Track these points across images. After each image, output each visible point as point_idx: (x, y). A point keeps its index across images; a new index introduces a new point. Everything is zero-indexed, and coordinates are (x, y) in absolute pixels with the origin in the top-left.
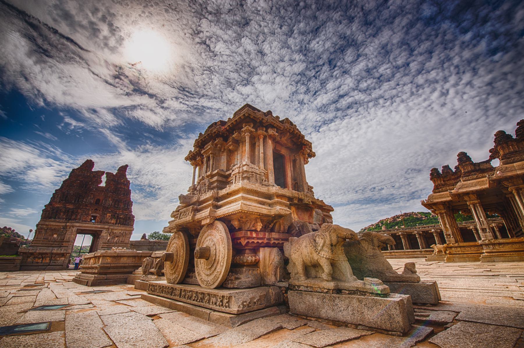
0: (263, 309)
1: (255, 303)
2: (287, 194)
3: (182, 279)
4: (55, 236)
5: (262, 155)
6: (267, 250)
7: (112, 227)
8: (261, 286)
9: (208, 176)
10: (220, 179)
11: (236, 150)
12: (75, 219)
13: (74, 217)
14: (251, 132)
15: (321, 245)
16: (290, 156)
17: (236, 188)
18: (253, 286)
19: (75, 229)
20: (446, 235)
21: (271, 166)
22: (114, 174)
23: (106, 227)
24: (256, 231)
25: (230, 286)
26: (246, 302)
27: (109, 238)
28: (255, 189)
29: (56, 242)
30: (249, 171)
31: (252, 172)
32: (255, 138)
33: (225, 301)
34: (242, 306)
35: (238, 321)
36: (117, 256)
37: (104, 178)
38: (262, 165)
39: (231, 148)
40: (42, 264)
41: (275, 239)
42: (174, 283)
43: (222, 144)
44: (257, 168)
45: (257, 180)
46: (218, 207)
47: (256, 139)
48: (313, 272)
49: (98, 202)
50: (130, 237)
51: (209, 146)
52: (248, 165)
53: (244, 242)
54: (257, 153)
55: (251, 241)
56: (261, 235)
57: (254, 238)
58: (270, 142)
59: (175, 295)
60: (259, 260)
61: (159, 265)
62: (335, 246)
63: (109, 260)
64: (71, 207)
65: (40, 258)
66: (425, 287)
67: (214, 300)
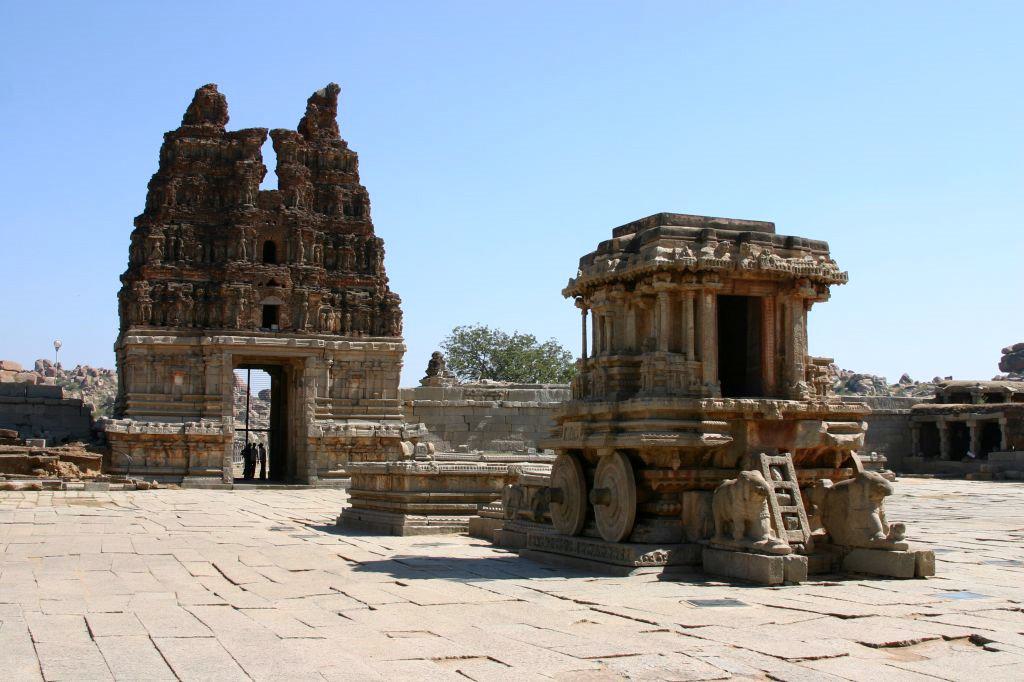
4: (178, 380)
5: (691, 333)
6: (694, 495)
10: (625, 370)
11: (651, 306)
13: (214, 314)
19: (226, 357)
24: (671, 469)
25: (638, 540)
37: (269, 155)
38: (691, 354)
41: (707, 479)
43: (624, 300)
46: (622, 431)
49: (270, 254)
51: (600, 295)
53: (655, 486)
55: (665, 484)
56: (683, 474)
57: (670, 479)
59: (571, 550)
60: (681, 511)
61: (536, 502)
65: (157, 451)
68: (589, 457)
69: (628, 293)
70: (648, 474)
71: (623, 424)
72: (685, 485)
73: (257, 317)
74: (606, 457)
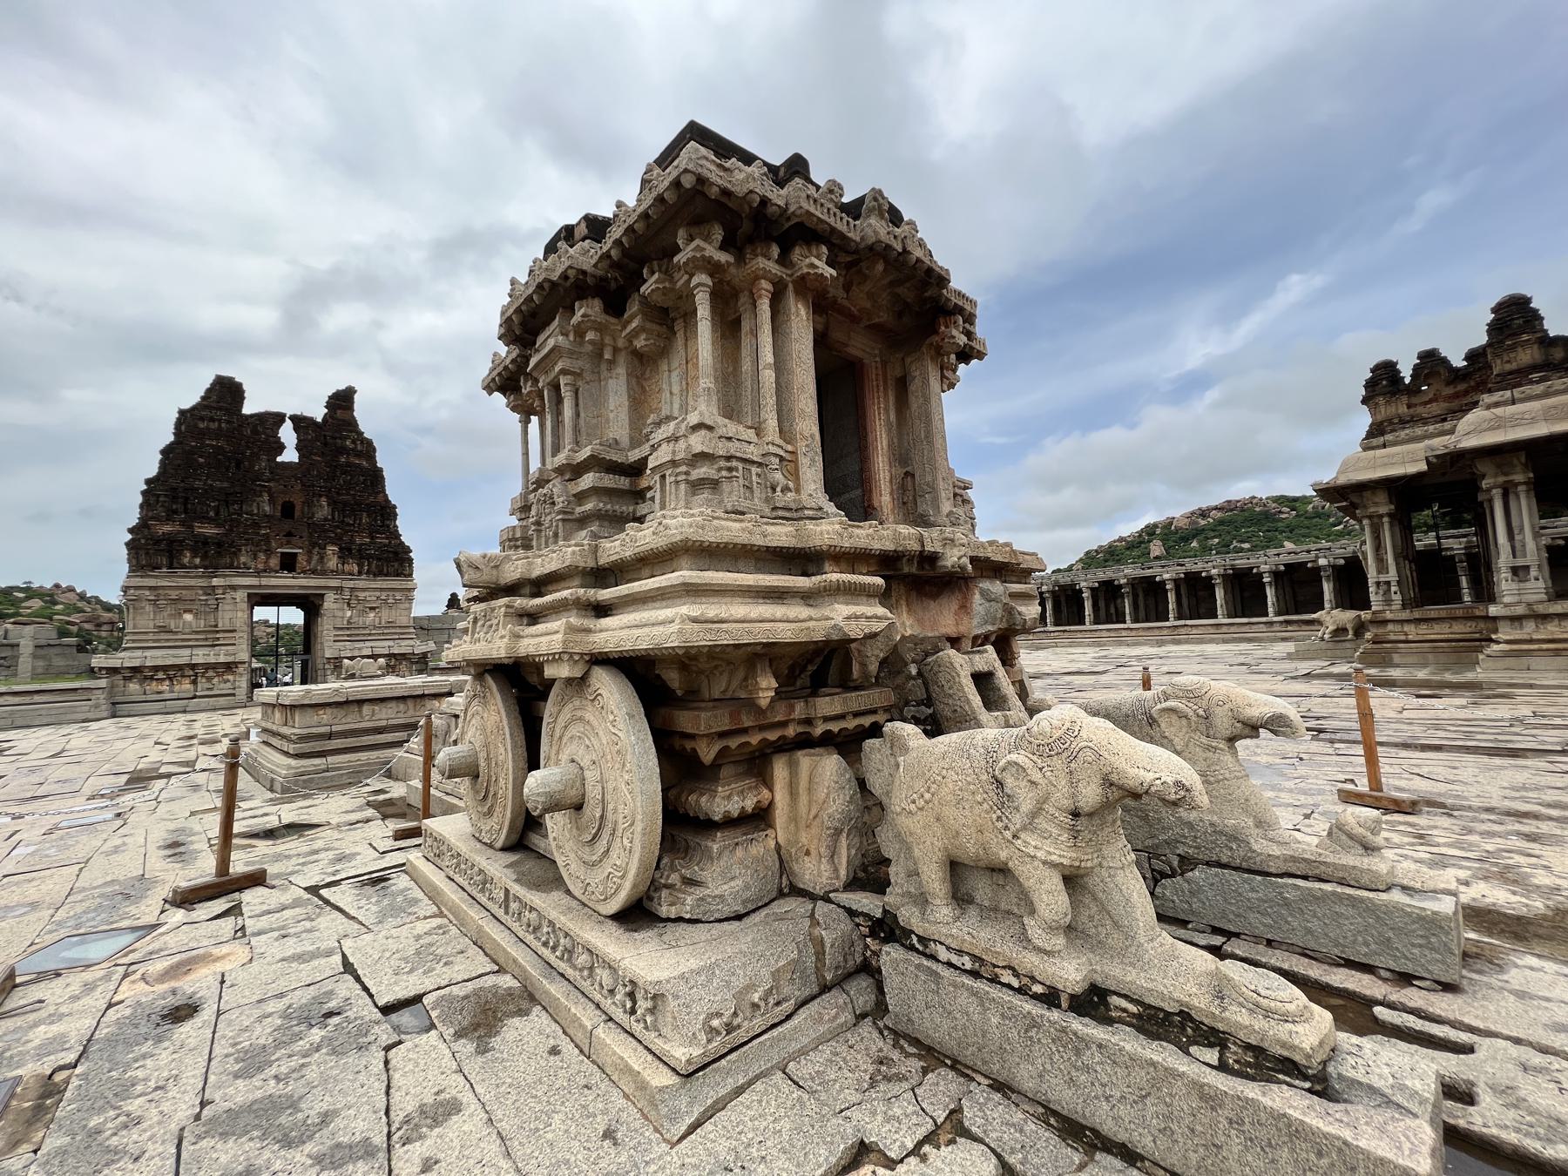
0: (789, 1017)
1: (755, 1006)
2: (877, 546)
3: (515, 837)
4: (188, 617)
5: (768, 376)
6: (805, 759)
7: (351, 584)
8: (781, 894)
9: (560, 471)
11: (664, 352)
12: (231, 566)
14: (714, 269)
15: (1026, 806)
16: (884, 364)
17: (660, 542)
18: (751, 907)
19: (241, 595)
20: (1378, 584)
21: (808, 424)
22: (319, 420)
23: (334, 583)
24: (751, 704)
26: (719, 1015)
27: (349, 614)
28: (744, 539)
29: (197, 633)
30: (730, 410)
31: (729, 458)
32: (735, 294)
33: (643, 1005)
34: (703, 1037)
35: (691, 1104)
36: (347, 702)
37: (287, 434)
38: (772, 423)
39: (640, 343)
40: (175, 695)
41: (826, 719)
42: (490, 846)
43: (600, 328)
44: (750, 435)
45: (749, 488)
47: (744, 299)
48: (982, 889)
49: (288, 510)
50: (410, 609)
51: (551, 339)
52: (710, 428)
53: (707, 753)
54: (746, 366)
55: (733, 743)
58: (803, 312)
60: (771, 803)
62: (1090, 815)
63: (325, 716)
64: (210, 531)
66: (1421, 918)
67: (603, 975)
68: (534, 680)
69: (613, 320)
70: (685, 721)
71: (606, 594)
72: (782, 738)
73: (274, 562)
74: (569, 681)
